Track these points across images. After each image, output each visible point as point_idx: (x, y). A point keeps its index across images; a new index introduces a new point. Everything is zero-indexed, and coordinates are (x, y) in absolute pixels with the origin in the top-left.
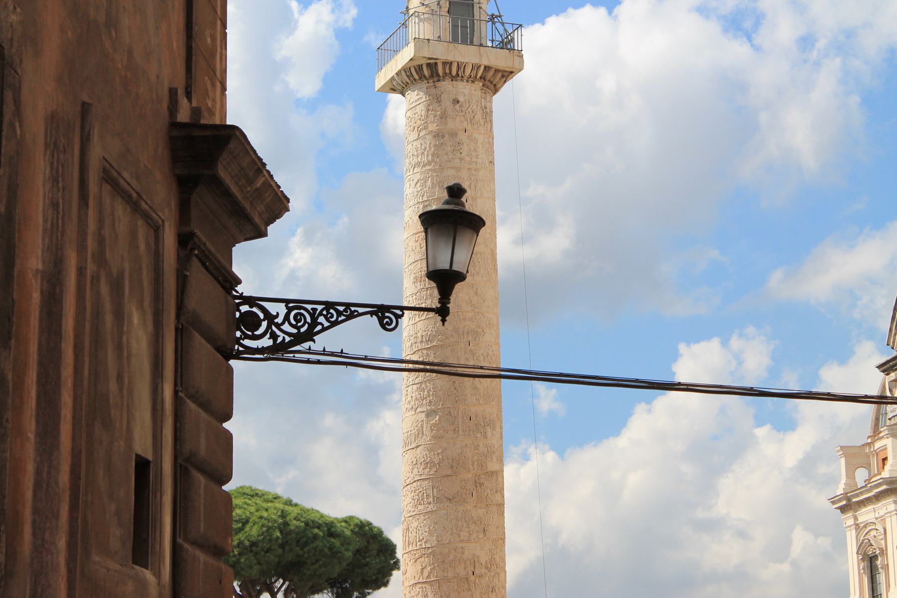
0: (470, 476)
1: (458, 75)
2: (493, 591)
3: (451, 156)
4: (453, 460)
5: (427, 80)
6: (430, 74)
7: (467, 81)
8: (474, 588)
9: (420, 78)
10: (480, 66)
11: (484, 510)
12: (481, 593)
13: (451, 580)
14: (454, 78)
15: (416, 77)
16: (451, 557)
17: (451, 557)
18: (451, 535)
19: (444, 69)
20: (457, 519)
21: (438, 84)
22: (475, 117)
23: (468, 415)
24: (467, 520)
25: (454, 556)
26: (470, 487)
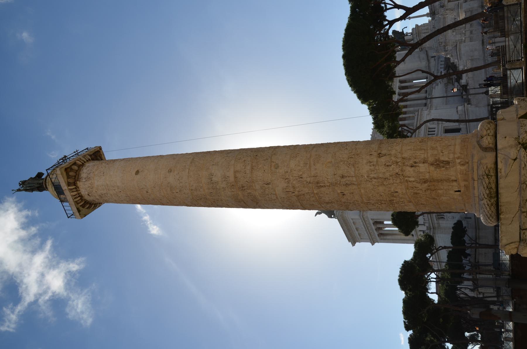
0: (240, 193)
1: (79, 196)
2: (301, 177)
8: (302, 192)
10: (69, 189)
11: (256, 184)
12: (304, 187)
14: (81, 197)
19: (80, 203)
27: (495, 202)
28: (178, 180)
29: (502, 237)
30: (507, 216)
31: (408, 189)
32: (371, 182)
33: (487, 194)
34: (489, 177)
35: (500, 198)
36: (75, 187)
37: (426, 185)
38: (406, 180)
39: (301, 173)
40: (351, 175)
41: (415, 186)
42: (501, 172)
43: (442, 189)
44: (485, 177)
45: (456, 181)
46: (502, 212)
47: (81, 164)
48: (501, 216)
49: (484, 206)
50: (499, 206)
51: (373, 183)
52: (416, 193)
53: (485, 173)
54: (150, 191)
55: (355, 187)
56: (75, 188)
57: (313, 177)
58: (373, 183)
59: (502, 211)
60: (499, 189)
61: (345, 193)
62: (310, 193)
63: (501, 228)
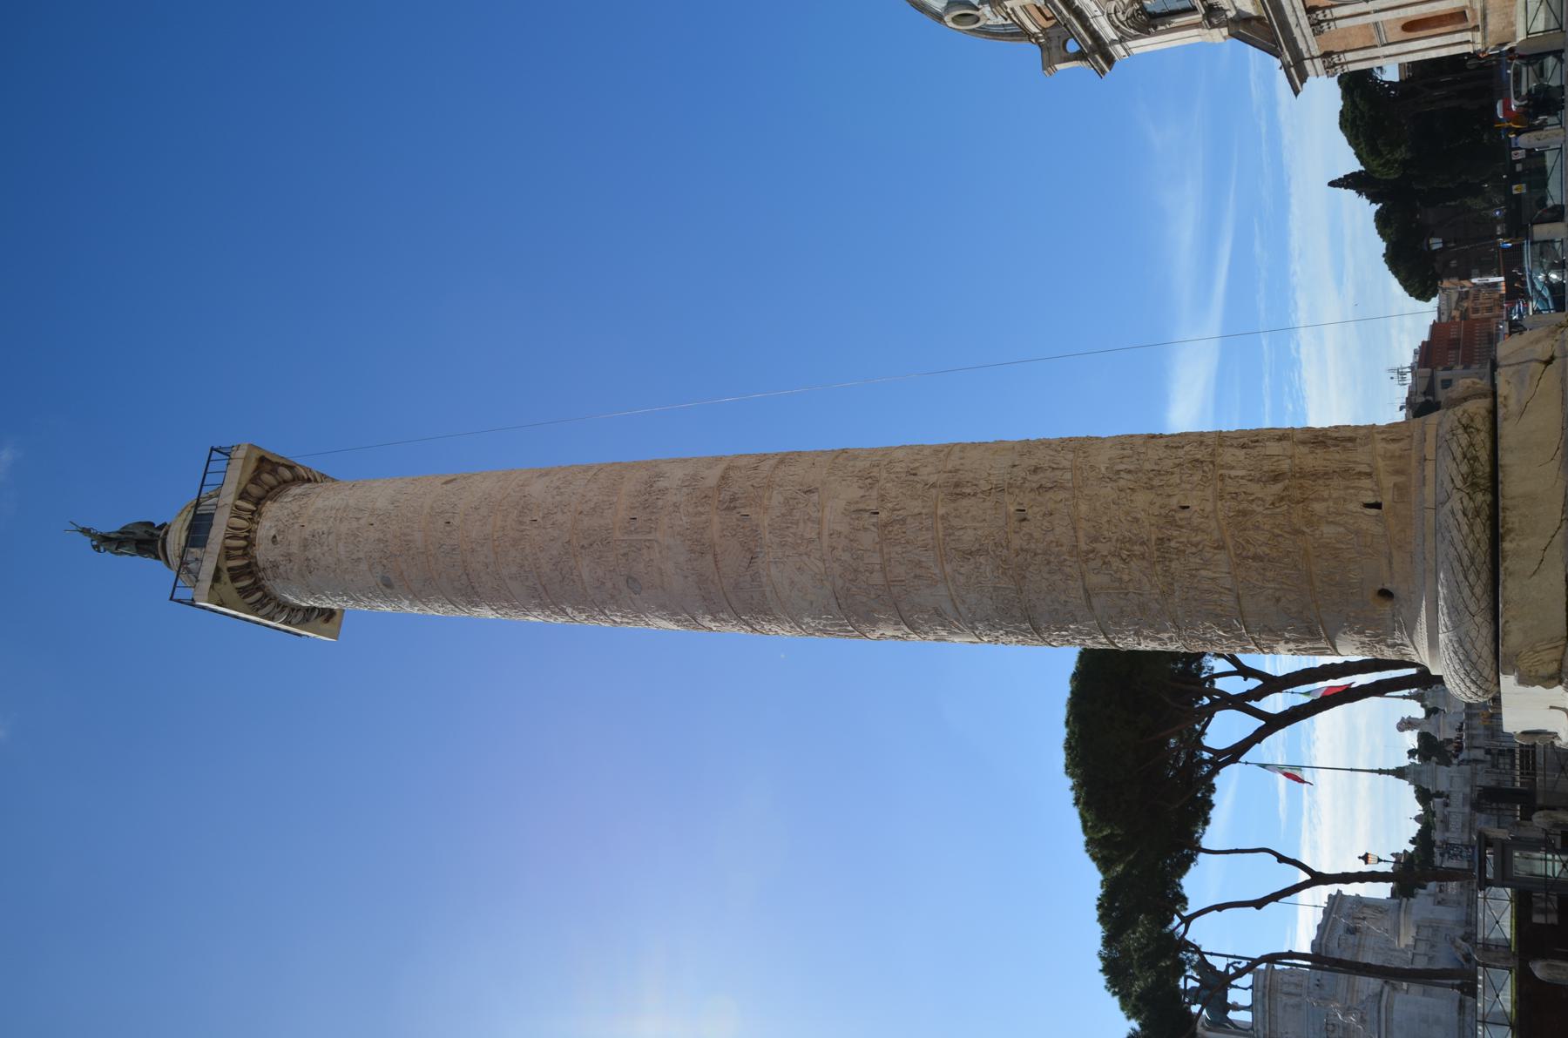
0: (716, 519)
1: (245, 538)
2: (914, 472)
3: (325, 548)
4: (692, 551)
5: (260, 580)
6: (248, 577)
7: (258, 523)
8: (901, 512)
9: (259, 589)
10: (236, 507)
13: (886, 557)
14: (250, 541)
15: (258, 595)
16: (846, 556)
17: (846, 556)
18: (809, 556)
20: (784, 545)
21: (261, 564)
22: (295, 511)
23: (629, 522)
24: (784, 525)
25: (844, 551)
26: (734, 520)
27: (1484, 506)
28: (558, 488)
29: (1507, 622)
30: (1524, 544)
31: (1221, 498)
32: (1115, 481)
33: (1462, 475)
34: (1472, 430)
35: (1502, 483)
36: (255, 509)
37: (1280, 486)
38: (1221, 475)
39: (918, 464)
40: (1061, 466)
41: (1244, 490)
42: (1505, 406)
43: (1325, 500)
44: (1460, 431)
45: (1369, 475)
46: (1510, 531)
47: (303, 477)
48: (1507, 545)
49: (1451, 521)
50: (1500, 510)
51: (1122, 483)
52: (1244, 513)
53: (1460, 422)
54: (456, 522)
55: (1062, 495)
56: (253, 512)
57: (950, 472)
58: (1122, 483)
59: (1510, 526)
60: (1500, 453)
61: (1030, 513)
62: (924, 517)
63: (1505, 588)
